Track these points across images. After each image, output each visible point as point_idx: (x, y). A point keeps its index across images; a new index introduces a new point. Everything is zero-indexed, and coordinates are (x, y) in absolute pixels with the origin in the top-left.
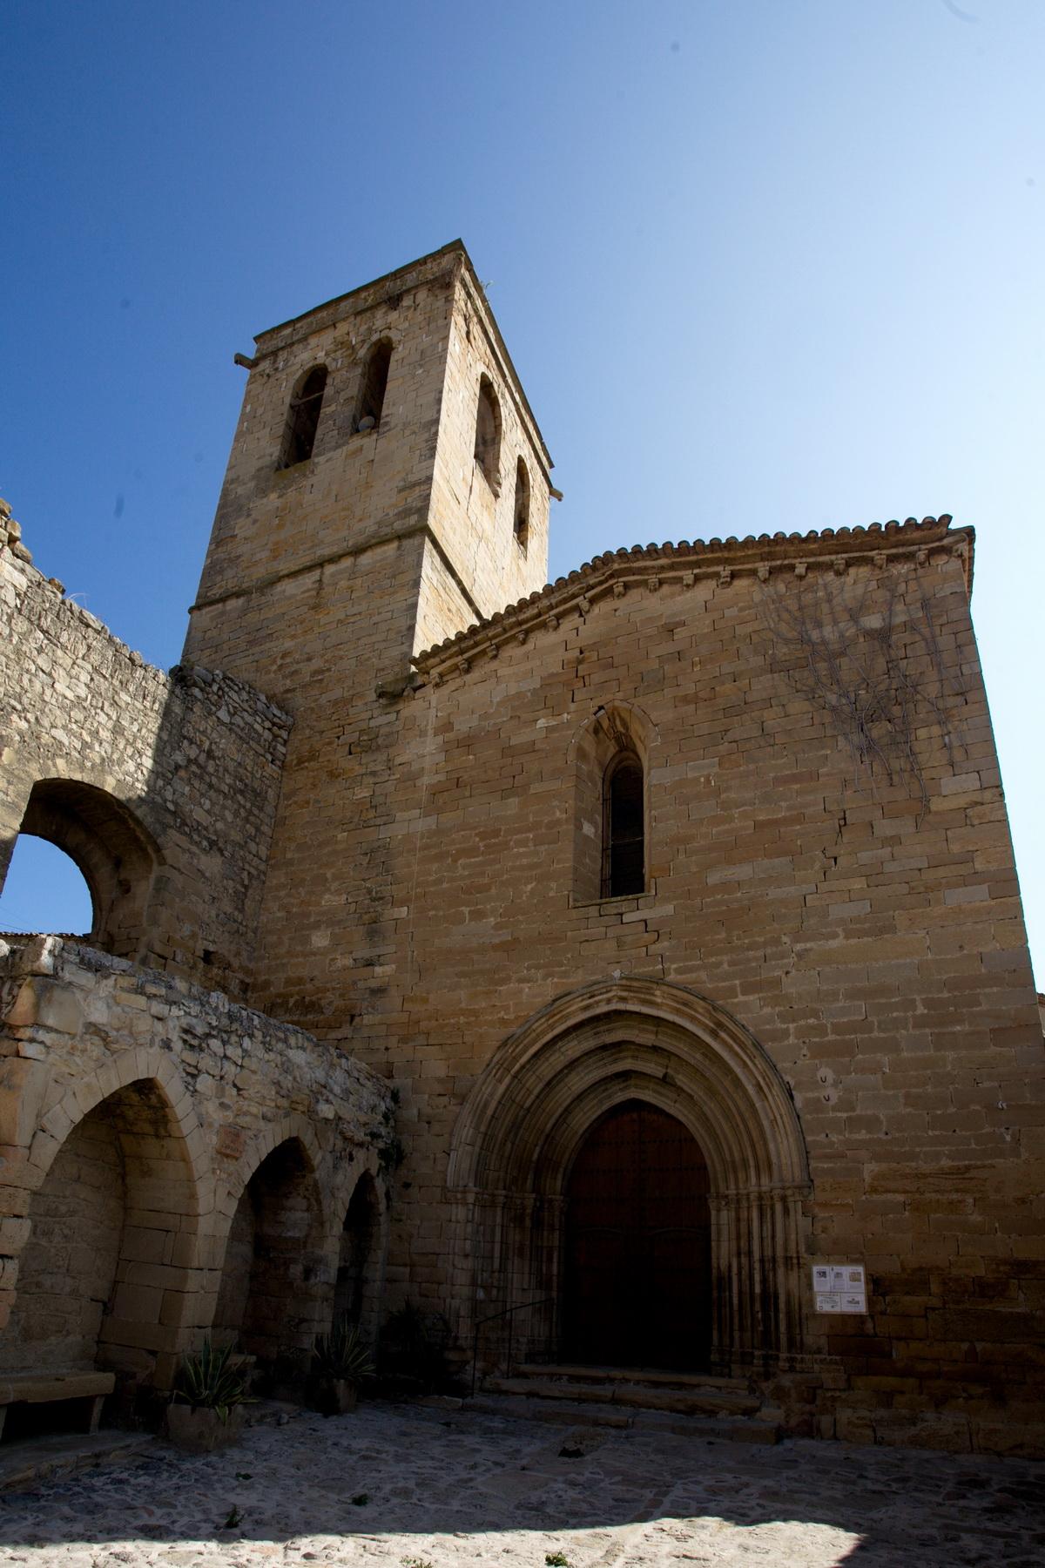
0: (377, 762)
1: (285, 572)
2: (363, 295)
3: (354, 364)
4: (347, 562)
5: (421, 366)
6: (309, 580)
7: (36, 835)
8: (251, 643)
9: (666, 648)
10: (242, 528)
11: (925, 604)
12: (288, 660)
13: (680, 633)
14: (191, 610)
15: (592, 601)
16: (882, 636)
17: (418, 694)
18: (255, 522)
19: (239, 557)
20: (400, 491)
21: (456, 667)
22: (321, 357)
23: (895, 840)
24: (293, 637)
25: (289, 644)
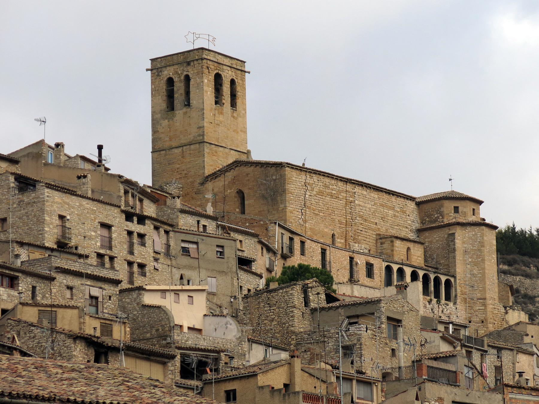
0: (201, 195)
1: (173, 146)
2: (180, 55)
3: (180, 81)
4: (188, 147)
5: (198, 89)
6: (180, 149)
7: (15, 152)
8: (169, 164)
9: (247, 178)
10: (161, 130)
11: (281, 176)
12: (179, 170)
13: (249, 175)
14: (151, 152)
15: (235, 167)
16: (275, 180)
17: (207, 182)
18: (163, 128)
19: (161, 138)
20: (198, 128)
21: (213, 178)
22: (171, 76)
23: (274, 214)
24: (179, 164)
25: (178, 166)
